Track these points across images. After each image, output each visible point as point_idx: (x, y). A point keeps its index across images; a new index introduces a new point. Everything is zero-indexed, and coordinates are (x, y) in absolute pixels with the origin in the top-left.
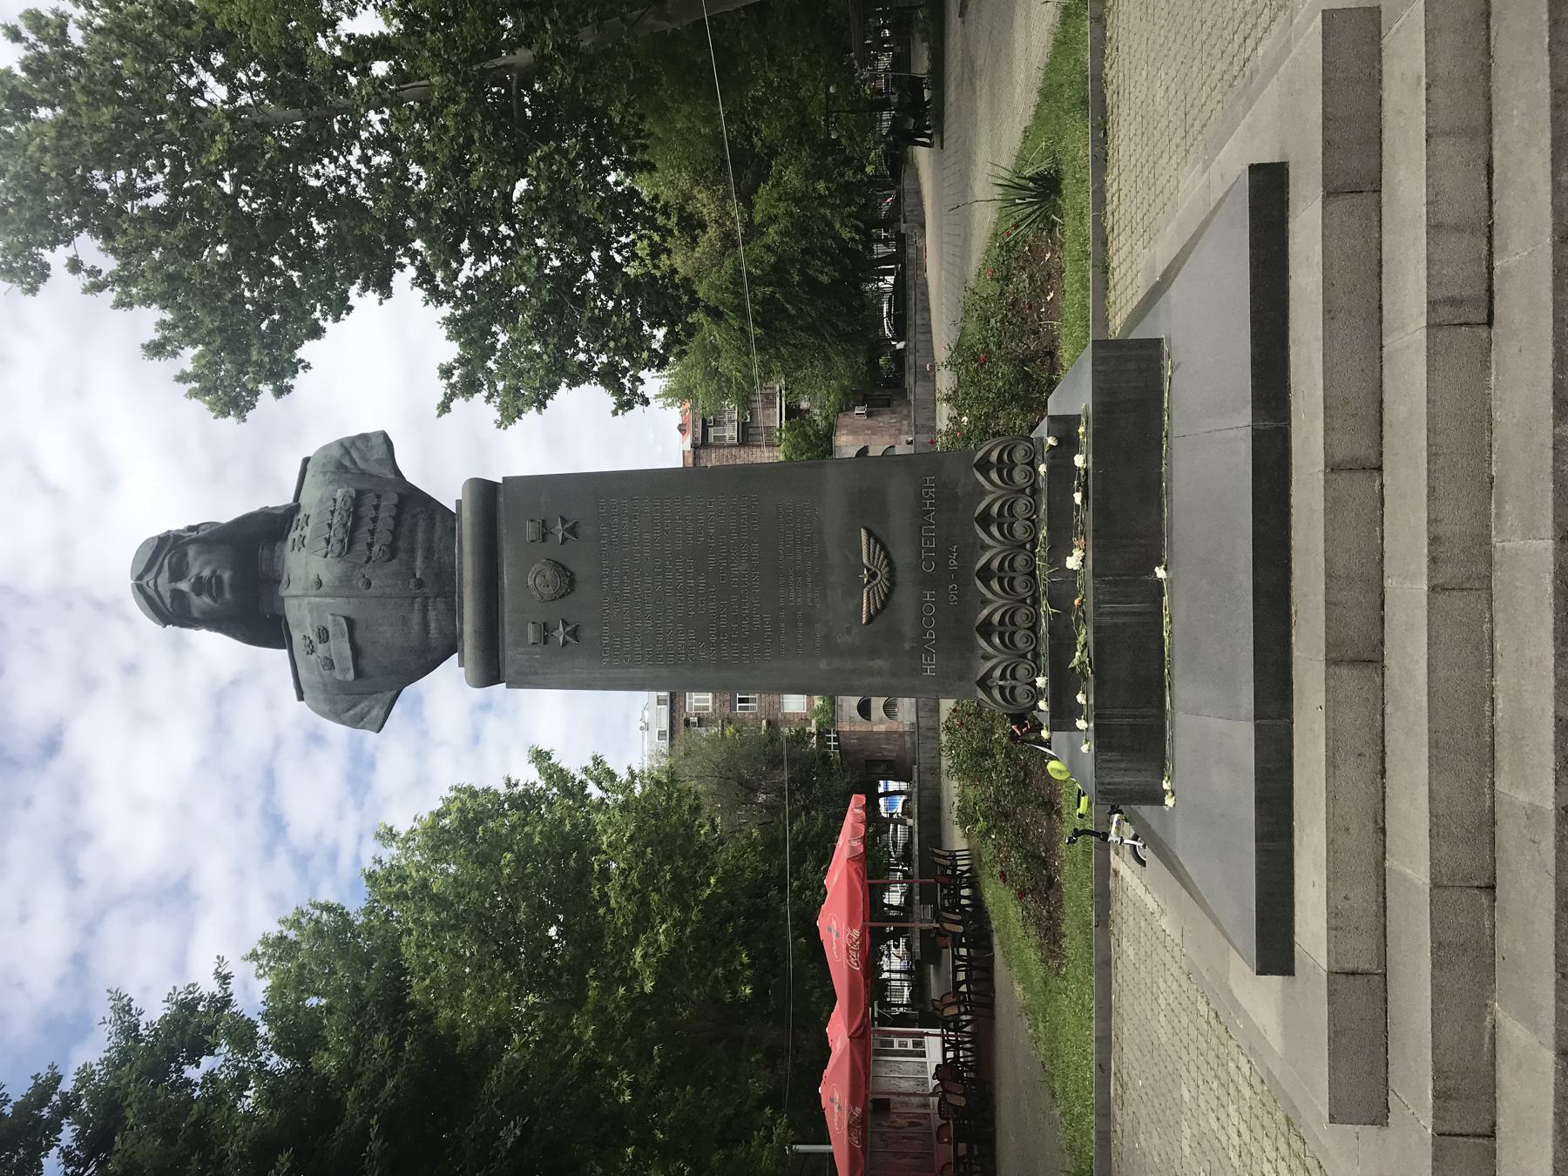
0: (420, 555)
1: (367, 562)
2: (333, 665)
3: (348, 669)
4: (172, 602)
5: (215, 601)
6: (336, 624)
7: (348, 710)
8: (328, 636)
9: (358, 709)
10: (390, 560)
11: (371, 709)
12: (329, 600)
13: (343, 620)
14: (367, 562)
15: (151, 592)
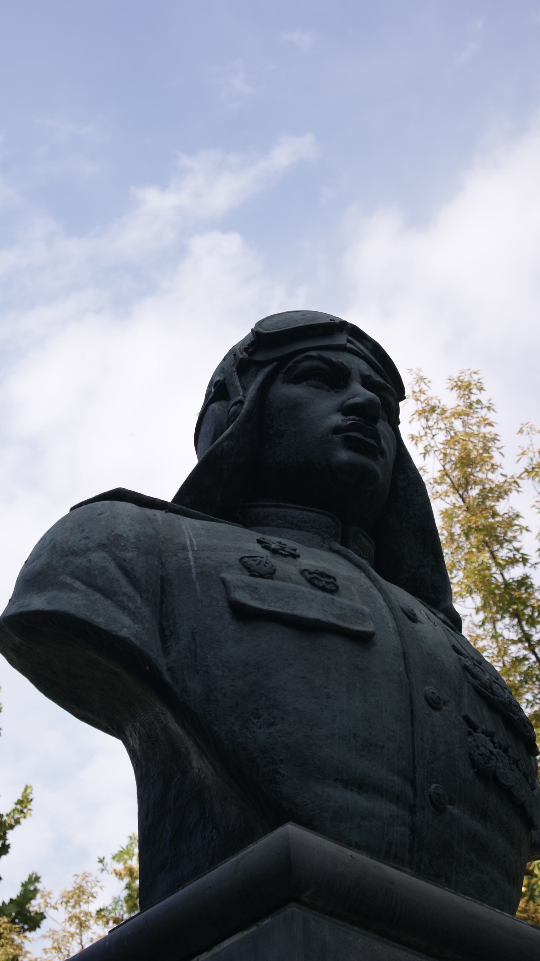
0: (478, 826)
1: (466, 719)
2: (261, 576)
3: (263, 601)
4: (329, 362)
5: (337, 430)
6: (360, 615)
7: (126, 573)
8: (323, 589)
9: (129, 590)
10: (474, 764)
11: (133, 615)
12: (392, 624)
13: (368, 627)
14: (466, 719)
15: (342, 339)
